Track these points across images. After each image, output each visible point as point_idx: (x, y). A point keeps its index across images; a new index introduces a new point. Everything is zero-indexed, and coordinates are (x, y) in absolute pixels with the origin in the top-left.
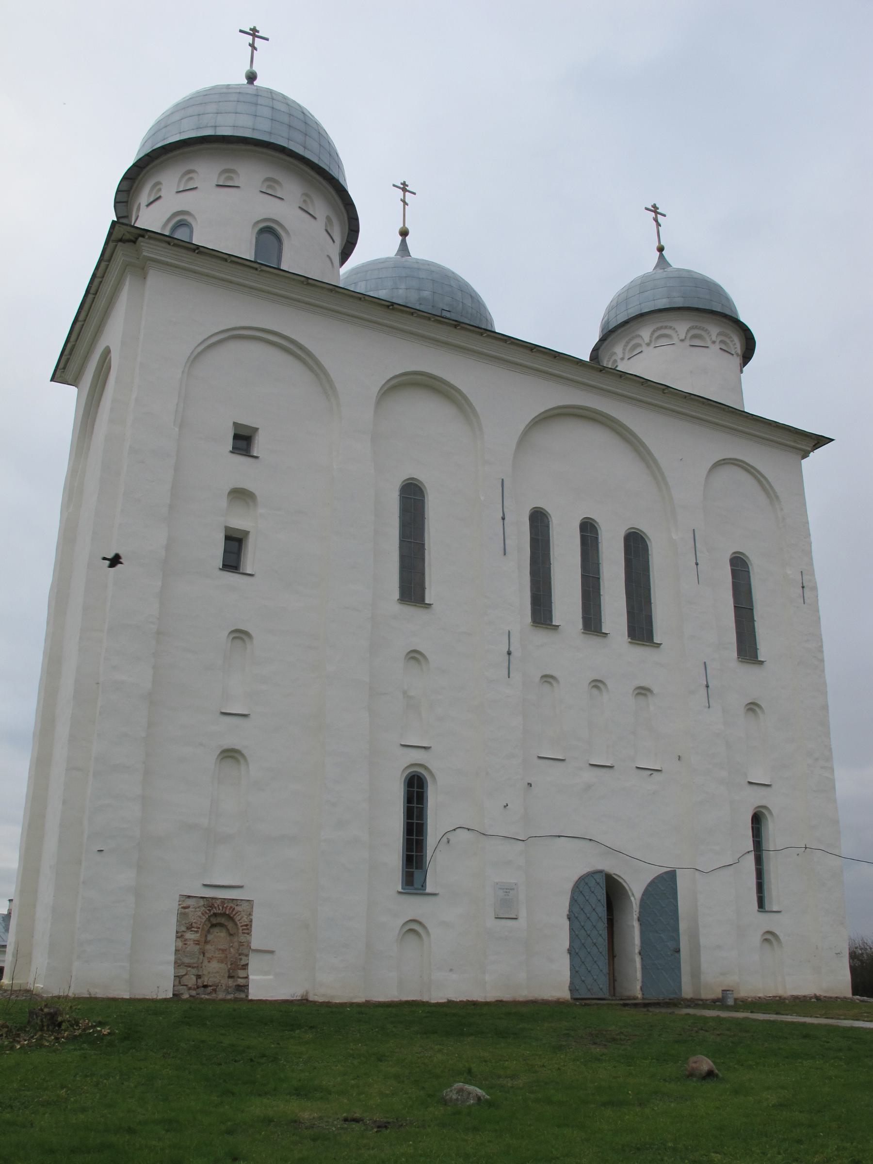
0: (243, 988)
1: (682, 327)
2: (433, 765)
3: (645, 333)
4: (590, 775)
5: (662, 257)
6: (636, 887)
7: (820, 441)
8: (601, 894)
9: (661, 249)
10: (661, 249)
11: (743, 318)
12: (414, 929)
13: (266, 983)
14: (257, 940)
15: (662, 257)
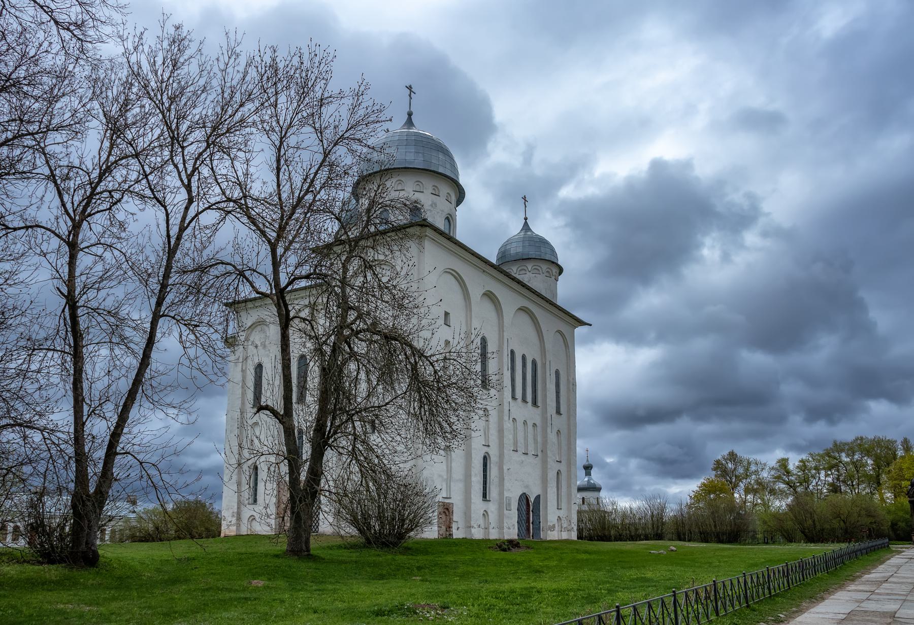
0: (451, 535)
1: (544, 267)
2: (490, 453)
3: (530, 266)
4: (523, 457)
5: (526, 224)
6: (532, 499)
7: (581, 323)
8: (525, 501)
9: (526, 219)
10: (526, 219)
11: (559, 263)
12: (486, 514)
13: (457, 534)
14: (455, 517)
15: (526, 224)
